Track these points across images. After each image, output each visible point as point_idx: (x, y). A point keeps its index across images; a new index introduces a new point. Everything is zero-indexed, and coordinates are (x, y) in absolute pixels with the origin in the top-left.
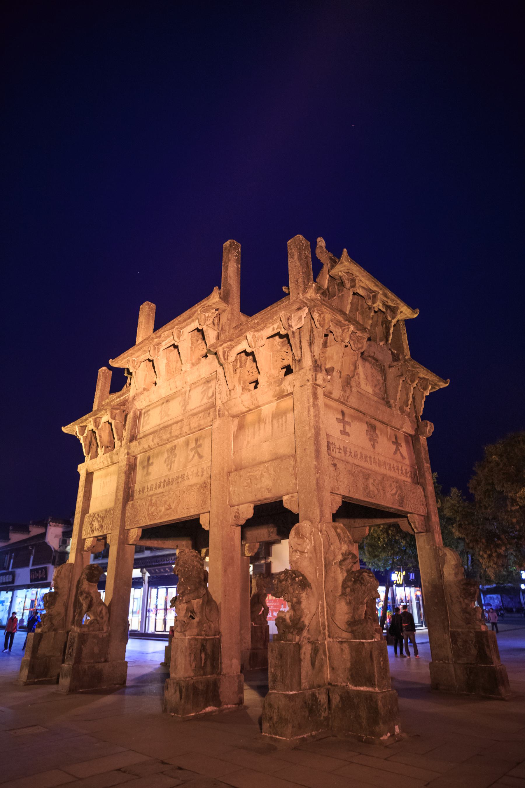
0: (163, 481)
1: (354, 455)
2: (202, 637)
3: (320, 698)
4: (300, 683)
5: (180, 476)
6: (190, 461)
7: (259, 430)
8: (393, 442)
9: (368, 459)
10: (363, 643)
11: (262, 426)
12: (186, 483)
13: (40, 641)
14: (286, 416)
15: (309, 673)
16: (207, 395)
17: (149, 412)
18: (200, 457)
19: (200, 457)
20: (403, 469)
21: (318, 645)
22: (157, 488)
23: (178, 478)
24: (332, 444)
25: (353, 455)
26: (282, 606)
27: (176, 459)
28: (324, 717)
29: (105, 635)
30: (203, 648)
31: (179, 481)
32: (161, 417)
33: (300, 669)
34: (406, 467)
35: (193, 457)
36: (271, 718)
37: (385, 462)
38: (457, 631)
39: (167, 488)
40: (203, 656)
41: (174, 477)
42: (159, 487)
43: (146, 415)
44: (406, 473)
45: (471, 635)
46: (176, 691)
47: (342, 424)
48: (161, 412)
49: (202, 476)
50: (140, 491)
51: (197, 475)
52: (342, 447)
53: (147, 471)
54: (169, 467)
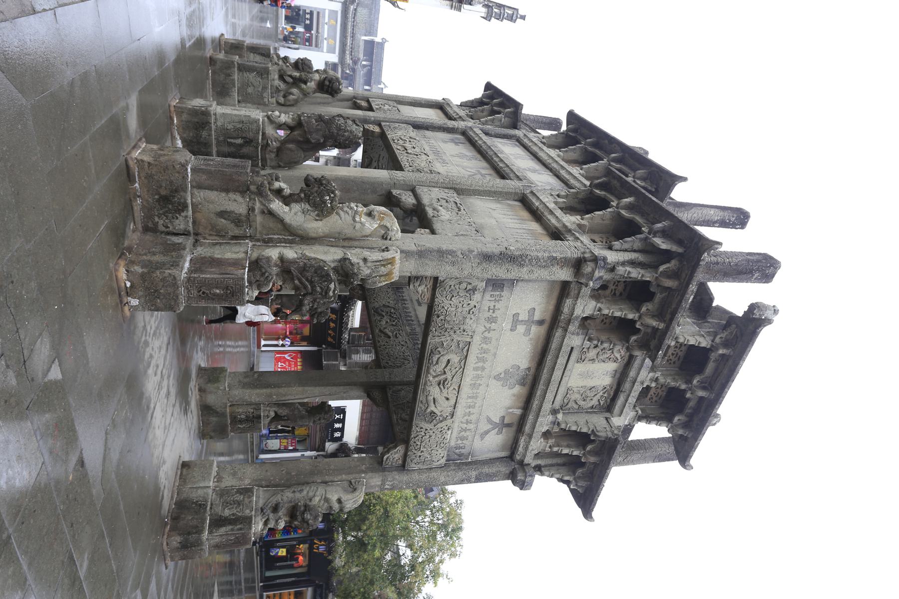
1: (486, 338)
2: (260, 141)
3: (180, 218)
4: (199, 186)
8: (504, 417)
9: (480, 364)
10: (245, 269)
13: (263, 55)
15: (211, 206)
20: (468, 433)
21: (245, 227)
24: (501, 296)
25: (486, 334)
28: (158, 222)
29: (266, 100)
30: (248, 142)
33: (217, 191)
34: (470, 438)
37: (476, 397)
38: (253, 496)
40: (239, 141)
44: (462, 439)
45: (248, 511)
47: (527, 319)
52: (497, 313)
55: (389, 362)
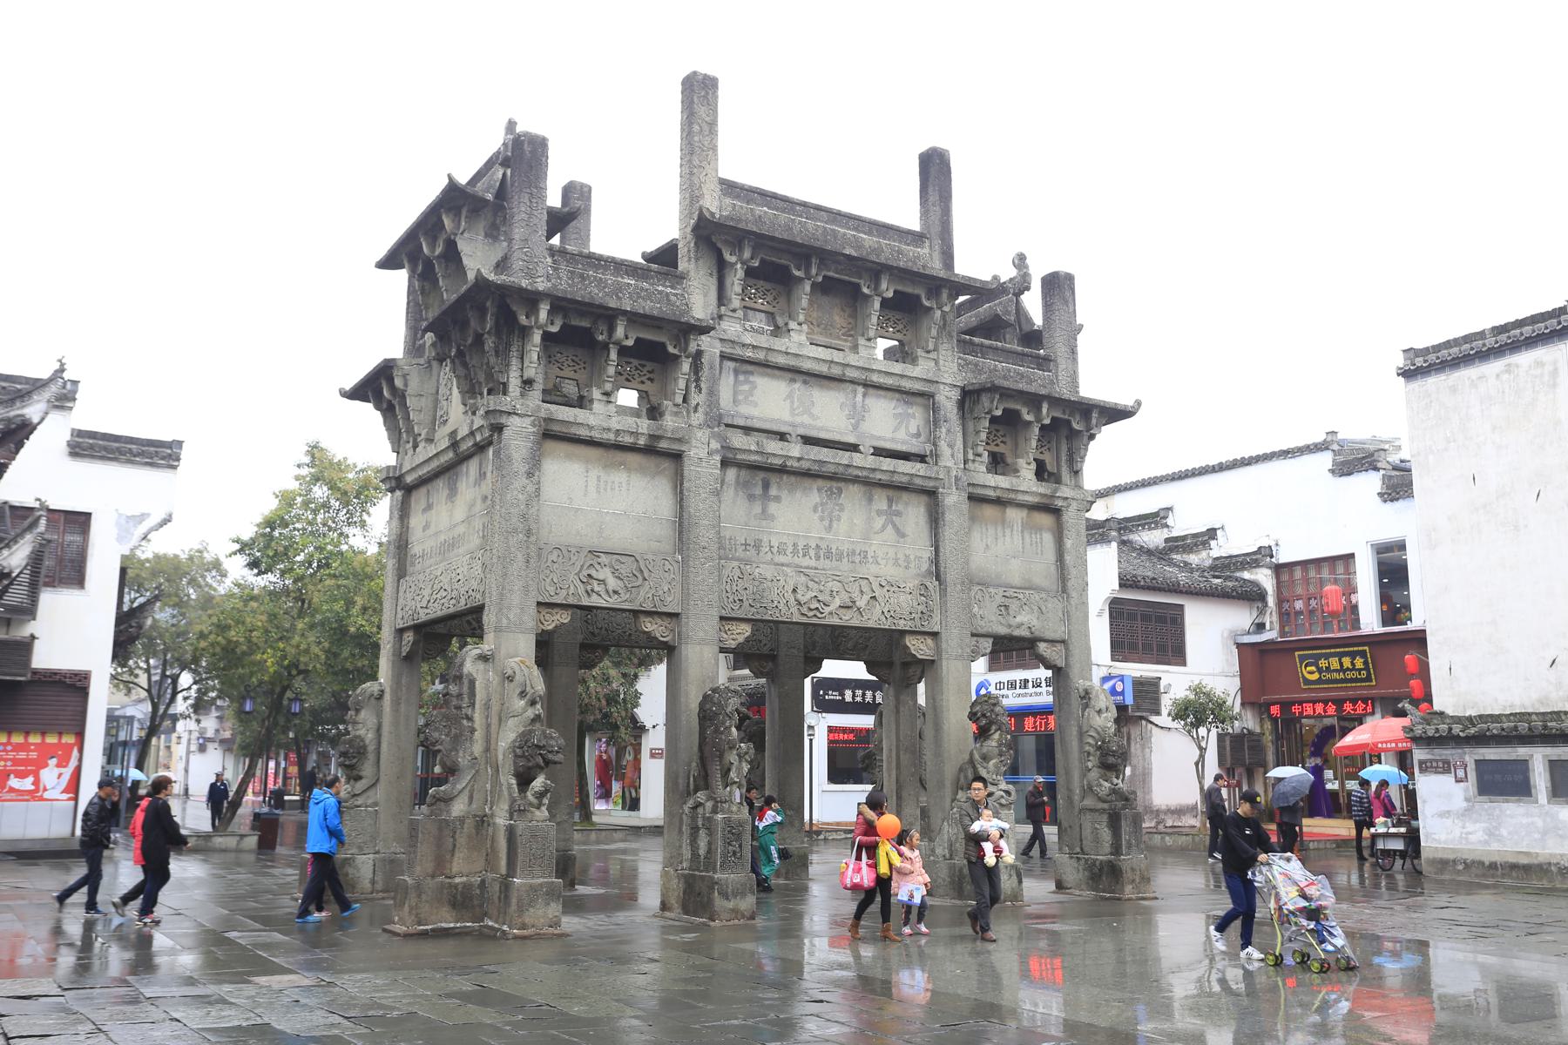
0: (814, 546)
5: (858, 552)
6: (875, 533)
7: (1004, 536)
11: (1008, 532)
12: (874, 569)
14: (1041, 535)
16: (907, 428)
17: (751, 378)
18: (901, 534)
19: (901, 534)
22: (801, 555)
23: (854, 552)
26: (53, 762)
27: (845, 516)
31: (857, 561)
32: (792, 410)
35: (884, 528)
36: (1133, 881)
39: (823, 563)
41: (845, 548)
42: (804, 555)
43: (741, 378)
46: (1011, 875)
48: (790, 396)
49: (906, 568)
50: (746, 545)
51: (896, 563)
53: (764, 511)
54: (826, 523)
55: (764, 642)
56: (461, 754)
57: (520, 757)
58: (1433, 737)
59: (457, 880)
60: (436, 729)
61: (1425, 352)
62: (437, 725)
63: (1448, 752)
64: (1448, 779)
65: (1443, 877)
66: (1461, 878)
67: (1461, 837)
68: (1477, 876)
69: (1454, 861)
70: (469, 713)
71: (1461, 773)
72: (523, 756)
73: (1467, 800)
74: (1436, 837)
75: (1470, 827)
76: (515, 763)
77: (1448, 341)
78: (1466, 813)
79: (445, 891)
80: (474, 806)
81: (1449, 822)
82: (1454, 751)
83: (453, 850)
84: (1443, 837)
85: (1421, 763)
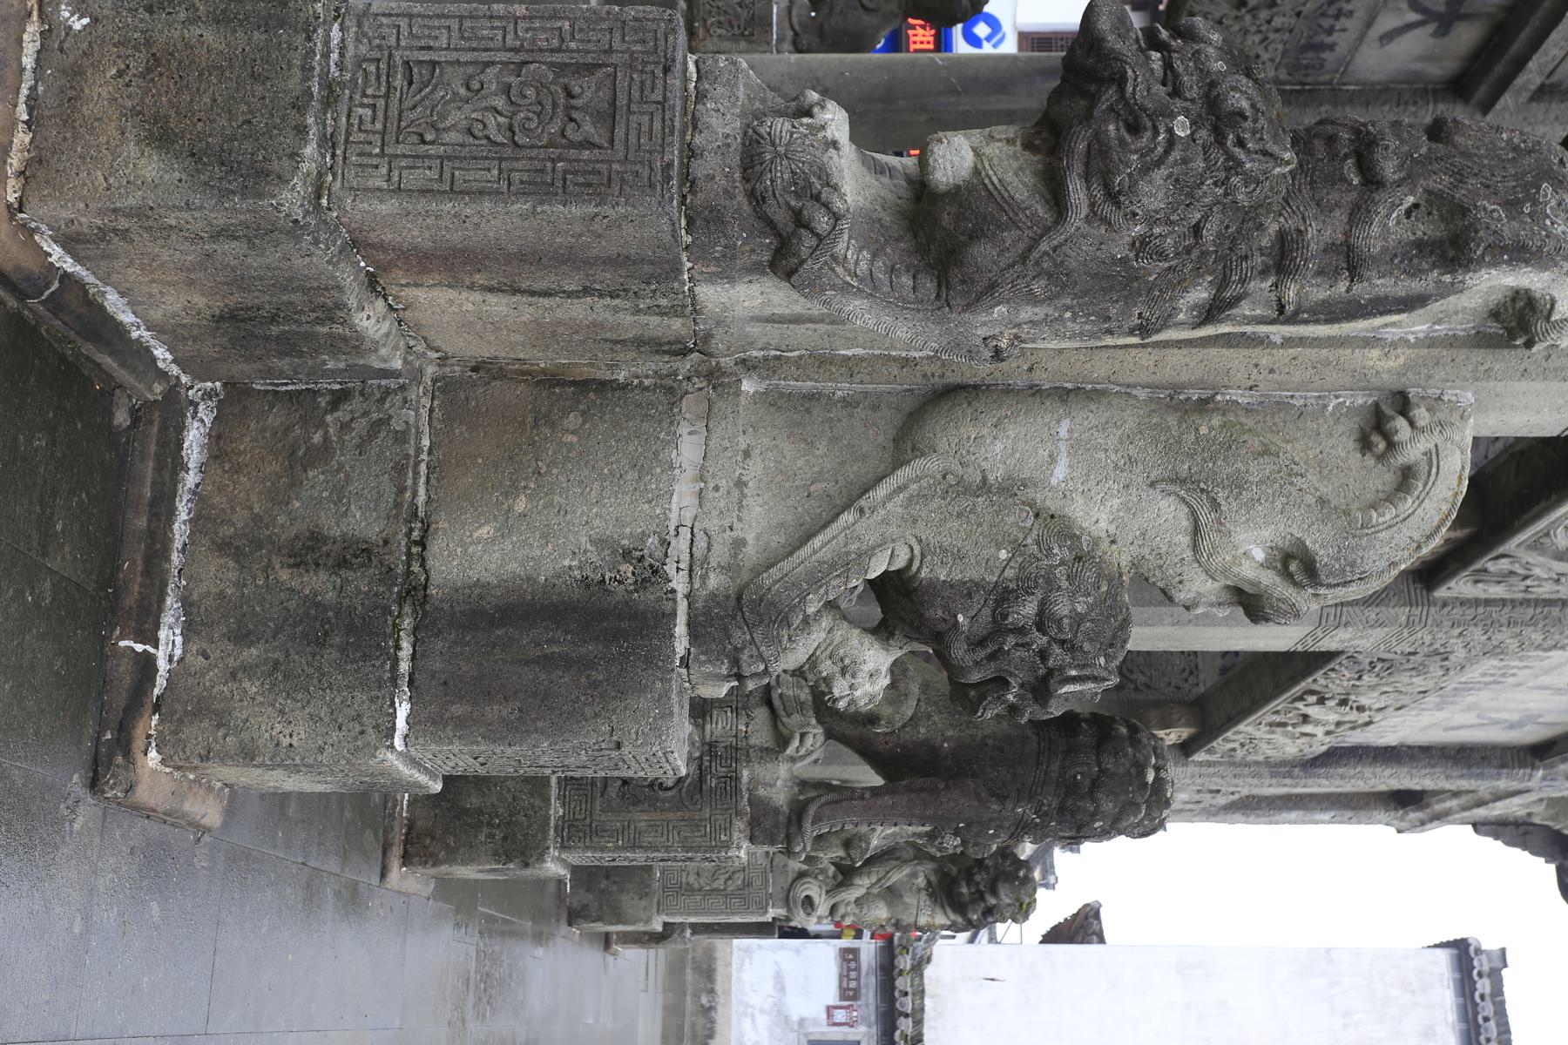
56: (1040, 312)
57: (999, 617)
58: (893, 988)
59: (370, 321)
60: (1185, 190)
61: (1495, 976)
62: (1210, 191)
63: (871, 999)
64: (831, 995)
65: (689, 971)
66: (689, 999)
67: (747, 1005)
68: (693, 1025)
69: (712, 991)
70: (1245, 309)
71: (840, 1016)
72: (999, 627)
73: (802, 1022)
74: (747, 966)
75: (763, 1021)
76: (968, 590)
77: (1508, 1031)
78: (781, 1017)
79: (296, 297)
80: (754, 330)
81: (768, 987)
82: (872, 1008)
83: (516, 291)
84: (746, 976)
85: (855, 952)
